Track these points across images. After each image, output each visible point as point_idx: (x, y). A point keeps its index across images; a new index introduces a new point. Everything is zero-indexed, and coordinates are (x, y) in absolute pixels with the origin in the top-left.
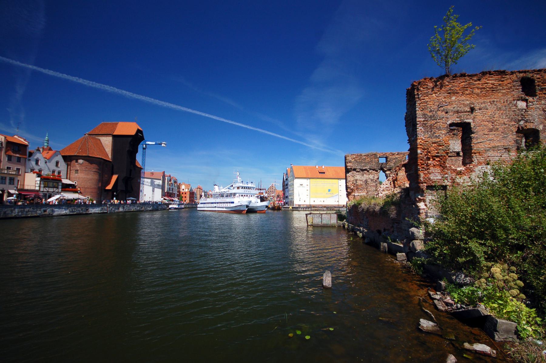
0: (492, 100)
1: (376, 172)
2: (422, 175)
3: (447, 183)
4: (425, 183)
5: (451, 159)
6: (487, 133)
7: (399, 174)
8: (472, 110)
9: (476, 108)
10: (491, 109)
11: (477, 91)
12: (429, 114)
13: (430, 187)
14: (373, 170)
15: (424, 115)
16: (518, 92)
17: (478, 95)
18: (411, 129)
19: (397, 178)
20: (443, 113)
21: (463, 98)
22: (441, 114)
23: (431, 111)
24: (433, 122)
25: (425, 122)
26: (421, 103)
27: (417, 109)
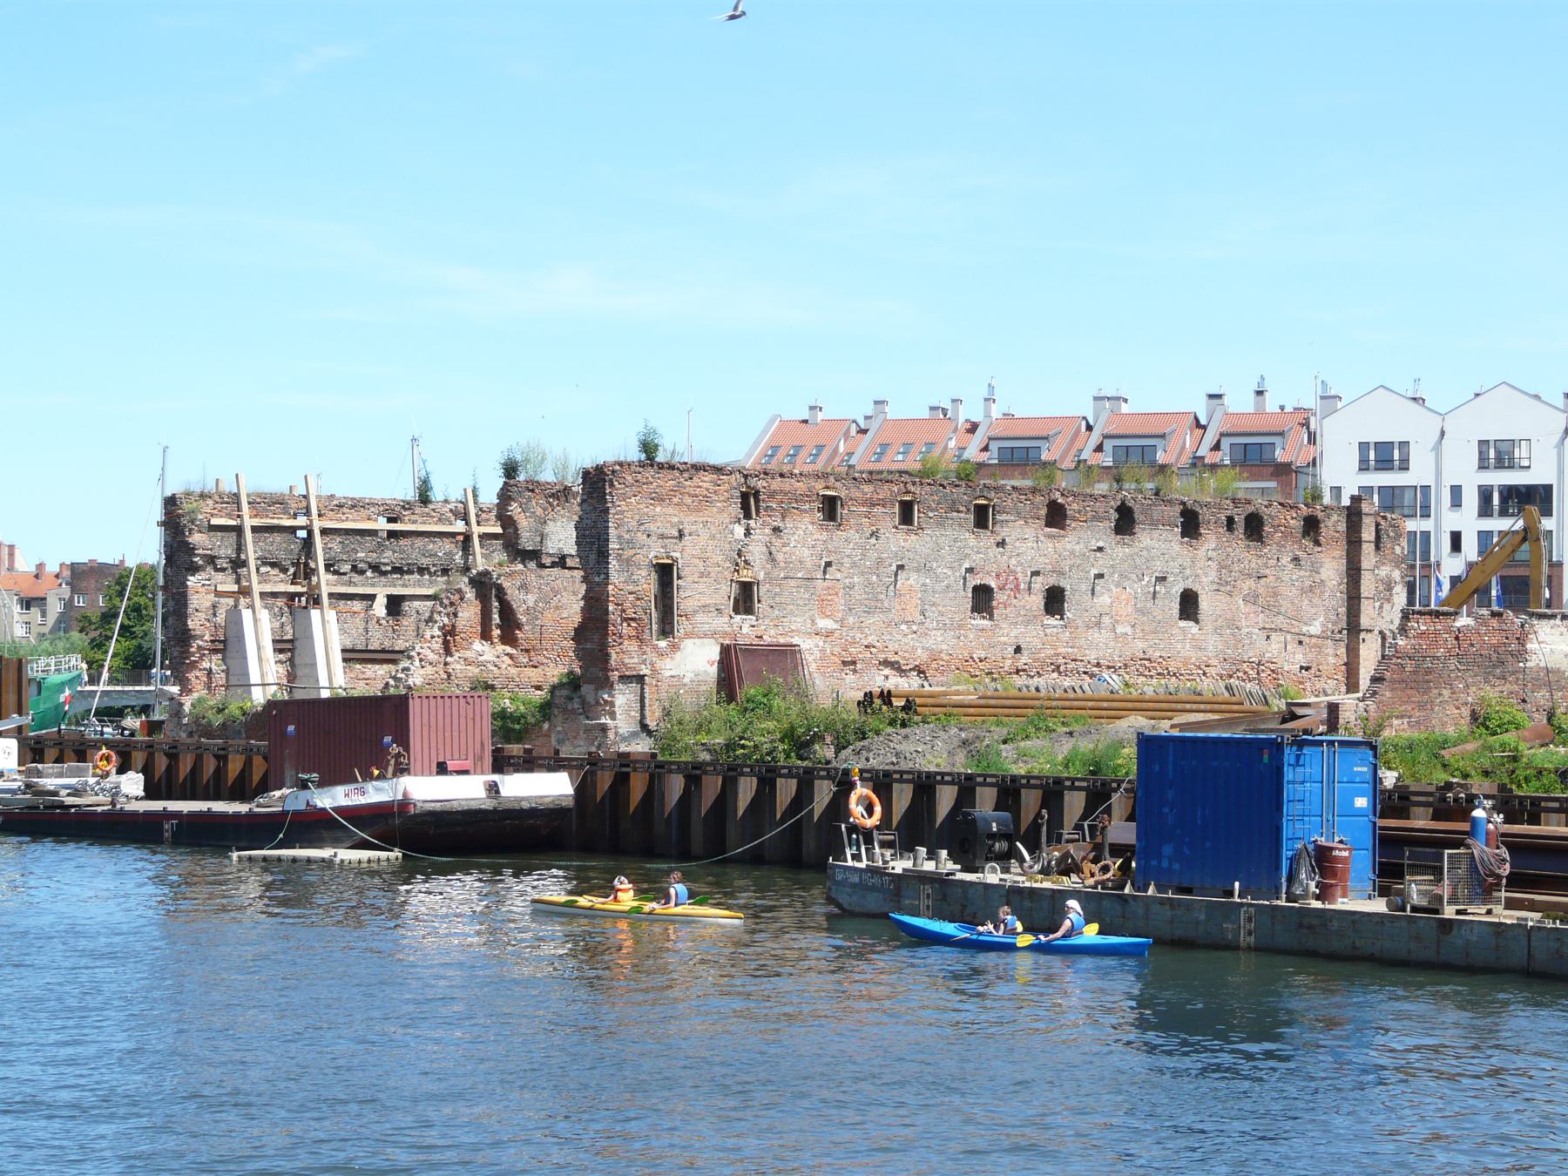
0: (705, 519)
1: (282, 575)
2: (614, 656)
3: (645, 671)
4: (617, 670)
6: (696, 580)
7: (460, 614)
8: (681, 535)
9: (686, 532)
10: (704, 534)
11: (688, 500)
12: (627, 536)
13: (624, 679)
14: (273, 565)
15: (619, 537)
16: (735, 509)
17: (688, 506)
18: (593, 557)
19: (453, 626)
20: (645, 537)
21: (670, 510)
22: (641, 537)
23: (628, 531)
24: (632, 552)
25: (621, 552)
26: (616, 514)
27: (610, 524)
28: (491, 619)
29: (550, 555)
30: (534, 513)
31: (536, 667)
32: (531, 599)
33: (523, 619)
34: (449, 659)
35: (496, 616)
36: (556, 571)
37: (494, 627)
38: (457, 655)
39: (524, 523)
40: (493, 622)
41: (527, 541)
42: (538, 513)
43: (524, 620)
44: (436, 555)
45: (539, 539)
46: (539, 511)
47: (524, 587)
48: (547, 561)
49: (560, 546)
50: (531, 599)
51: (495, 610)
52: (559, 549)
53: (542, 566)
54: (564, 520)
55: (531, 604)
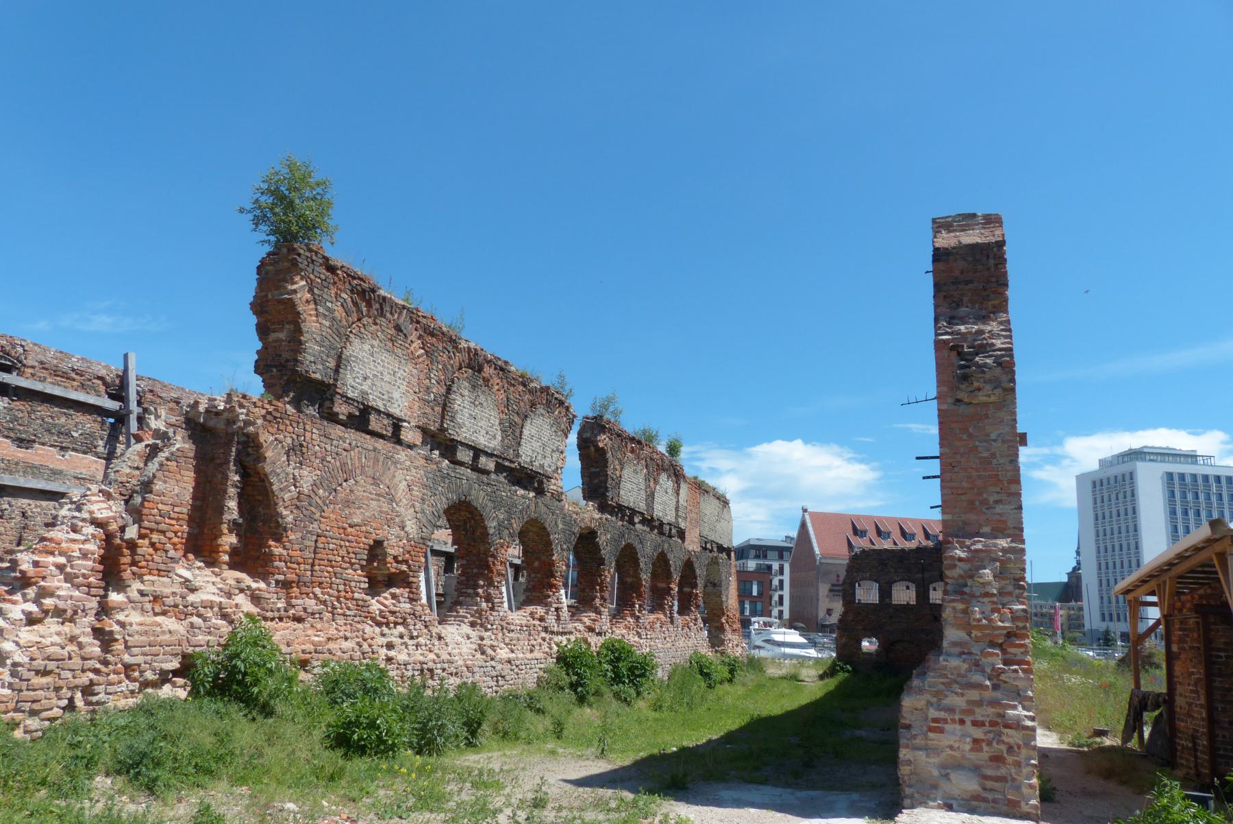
5: (375, 450)
28: (220, 510)
29: (348, 400)
30: (329, 309)
31: (299, 620)
32: (307, 477)
33: (288, 516)
34: (115, 597)
35: (232, 504)
36: (352, 436)
37: (225, 528)
38: (136, 585)
39: (313, 325)
40: (227, 517)
41: (314, 363)
42: (337, 314)
43: (290, 519)
44: (68, 434)
45: (332, 364)
46: (339, 313)
47: (297, 450)
48: (342, 409)
49: (365, 388)
50: (307, 477)
51: (232, 491)
52: (364, 393)
53: (332, 418)
54: (376, 343)
55: (306, 487)
